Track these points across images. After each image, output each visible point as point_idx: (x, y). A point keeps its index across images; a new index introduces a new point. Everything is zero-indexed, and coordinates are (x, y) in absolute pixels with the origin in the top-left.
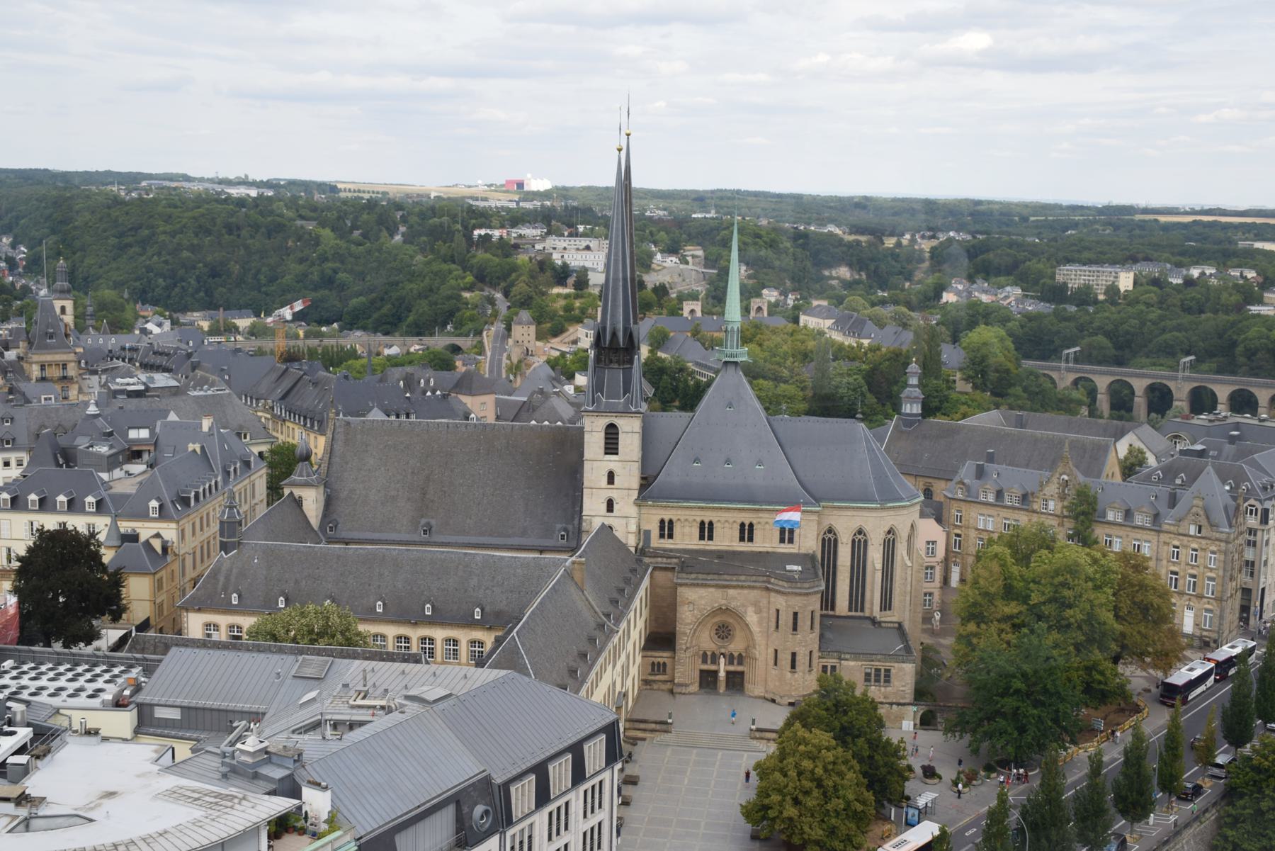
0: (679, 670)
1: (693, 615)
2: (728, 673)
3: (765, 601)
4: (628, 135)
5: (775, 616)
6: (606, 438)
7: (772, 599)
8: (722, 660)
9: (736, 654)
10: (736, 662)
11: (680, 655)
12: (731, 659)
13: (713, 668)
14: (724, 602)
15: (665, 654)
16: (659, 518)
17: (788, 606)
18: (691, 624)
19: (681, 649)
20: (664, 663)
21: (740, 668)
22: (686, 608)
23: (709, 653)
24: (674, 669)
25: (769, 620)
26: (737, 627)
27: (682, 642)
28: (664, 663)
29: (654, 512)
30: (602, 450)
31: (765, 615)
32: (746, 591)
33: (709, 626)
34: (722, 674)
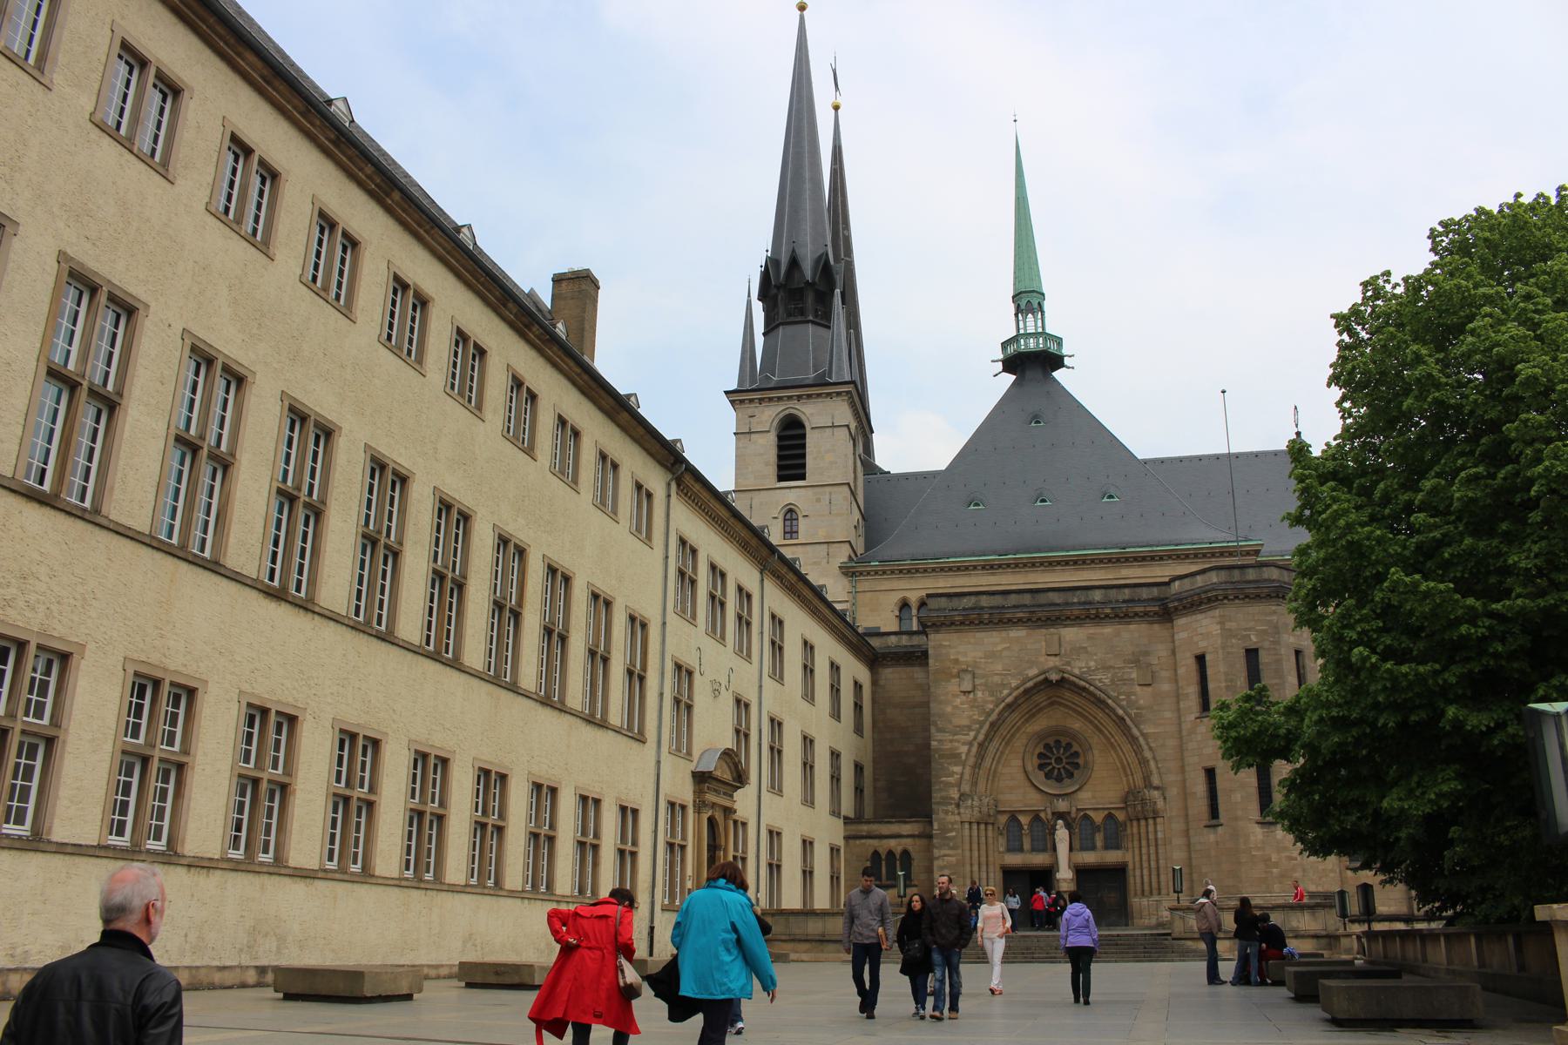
0: (945, 858)
1: (974, 704)
2: (1081, 872)
3: (1161, 651)
4: (836, 108)
5: (1194, 676)
6: (780, 448)
7: (1181, 636)
8: (1062, 834)
9: (1098, 817)
10: (1099, 840)
11: (946, 817)
12: (1084, 831)
13: (1039, 859)
14: (1053, 662)
15: (906, 829)
16: (895, 598)
17: (1227, 634)
18: (969, 728)
19: (946, 801)
20: (906, 853)
21: (1112, 857)
22: (953, 686)
23: (1024, 820)
24: (930, 870)
25: (1178, 697)
26: (1095, 740)
27: (952, 778)
28: (906, 853)
29: (886, 585)
30: (772, 471)
31: (1166, 687)
32: (1107, 630)
33: (1020, 742)
34: (1065, 875)
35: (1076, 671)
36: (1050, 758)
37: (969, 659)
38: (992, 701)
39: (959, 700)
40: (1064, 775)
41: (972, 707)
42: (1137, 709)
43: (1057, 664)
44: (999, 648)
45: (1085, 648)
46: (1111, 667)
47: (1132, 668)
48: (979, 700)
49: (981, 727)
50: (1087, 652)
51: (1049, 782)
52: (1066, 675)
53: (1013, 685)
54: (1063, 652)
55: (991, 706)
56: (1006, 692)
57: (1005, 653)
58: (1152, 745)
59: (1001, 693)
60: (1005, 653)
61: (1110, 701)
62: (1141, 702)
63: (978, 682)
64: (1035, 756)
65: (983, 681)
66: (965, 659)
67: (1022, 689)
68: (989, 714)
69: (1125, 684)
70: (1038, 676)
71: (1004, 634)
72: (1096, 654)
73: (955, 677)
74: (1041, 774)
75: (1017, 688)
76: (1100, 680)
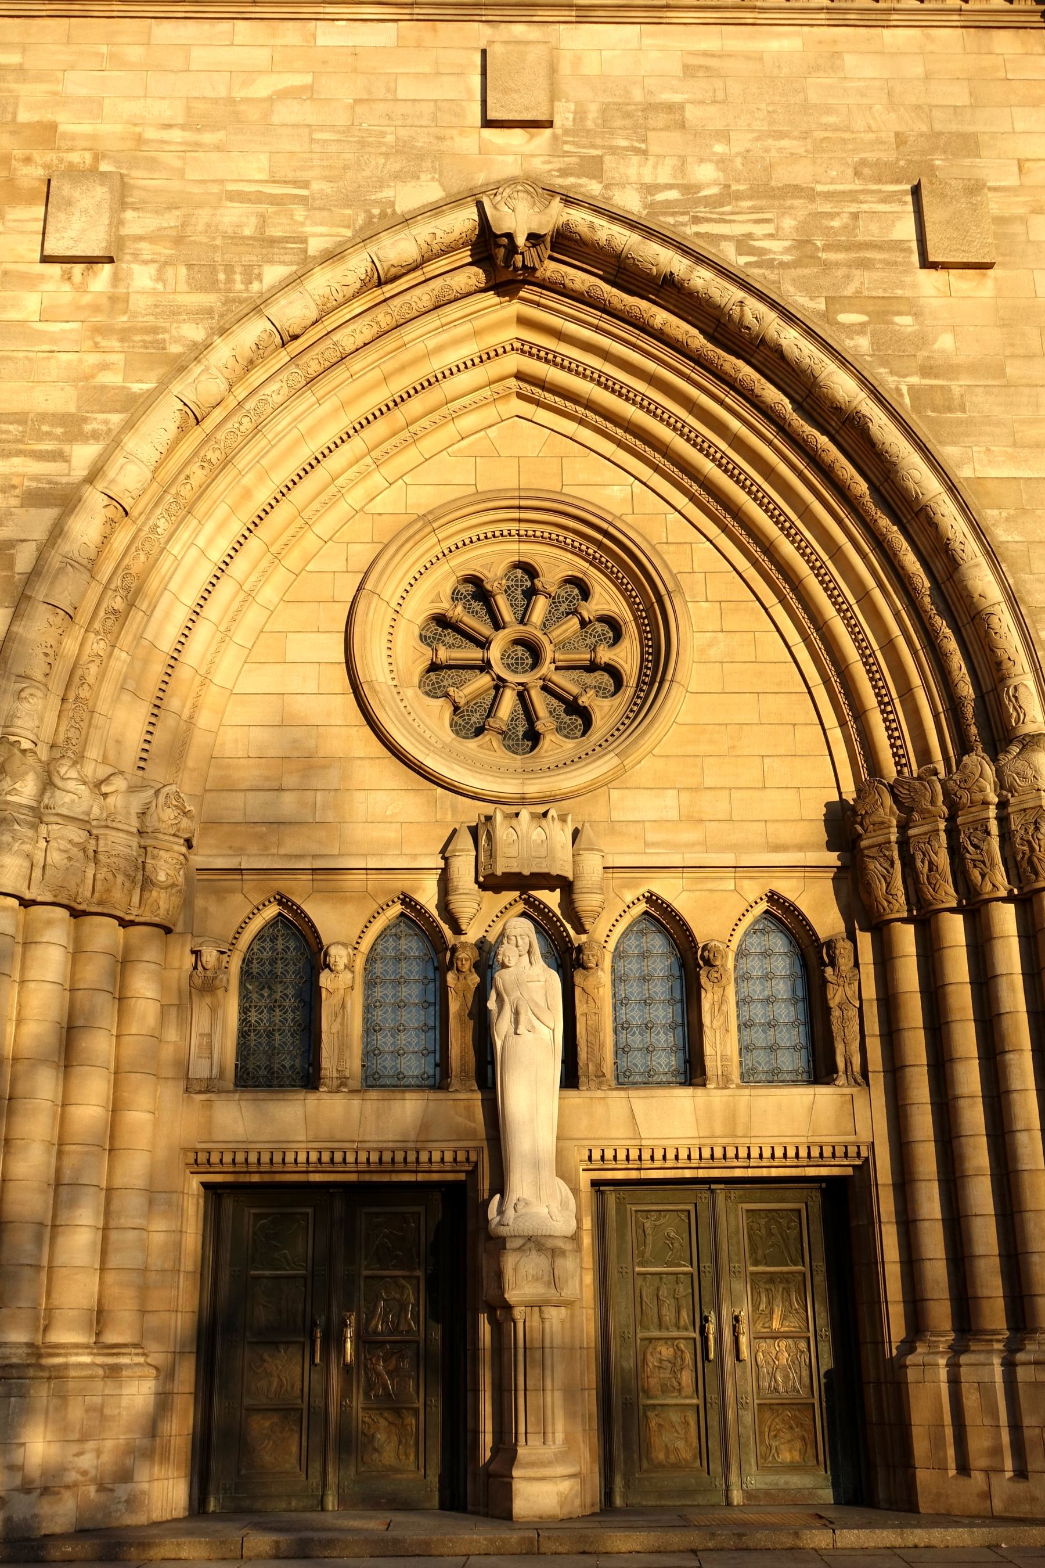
35: (630, 202)
36: (484, 644)
37: (104, 128)
38: (209, 312)
39: (30, 304)
40: (545, 722)
41: (98, 330)
42: (926, 371)
43: (539, 165)
44: (263, 88)
45: (670, 108)
46: (795, 190)
47: (887, 198)
48: (139, 303)
49: (130, 425)
50: (682, 126)
51: (472, 744)
52: (580, 219)
53: (315, 246)
54: (563, 118)
55: (195, 332)
56: (273, 274)
57: (287, 113)
58: (1002, 534)
59: (251, 274)
60: (287, 113)
61: (790, 339)
62: (945, 342)
63: (135, 223)
64: (408, 634)
65: (170, 220)
66: (86, 128)
67: (357, 265)
68: (179, 367)
69: (865, 264)
70: (435, 209)
71: (291, 34)
72: (724, 136)
73: (14, 194)
74: (438, 712)
75: (333, 256)
76: (743, 244)
